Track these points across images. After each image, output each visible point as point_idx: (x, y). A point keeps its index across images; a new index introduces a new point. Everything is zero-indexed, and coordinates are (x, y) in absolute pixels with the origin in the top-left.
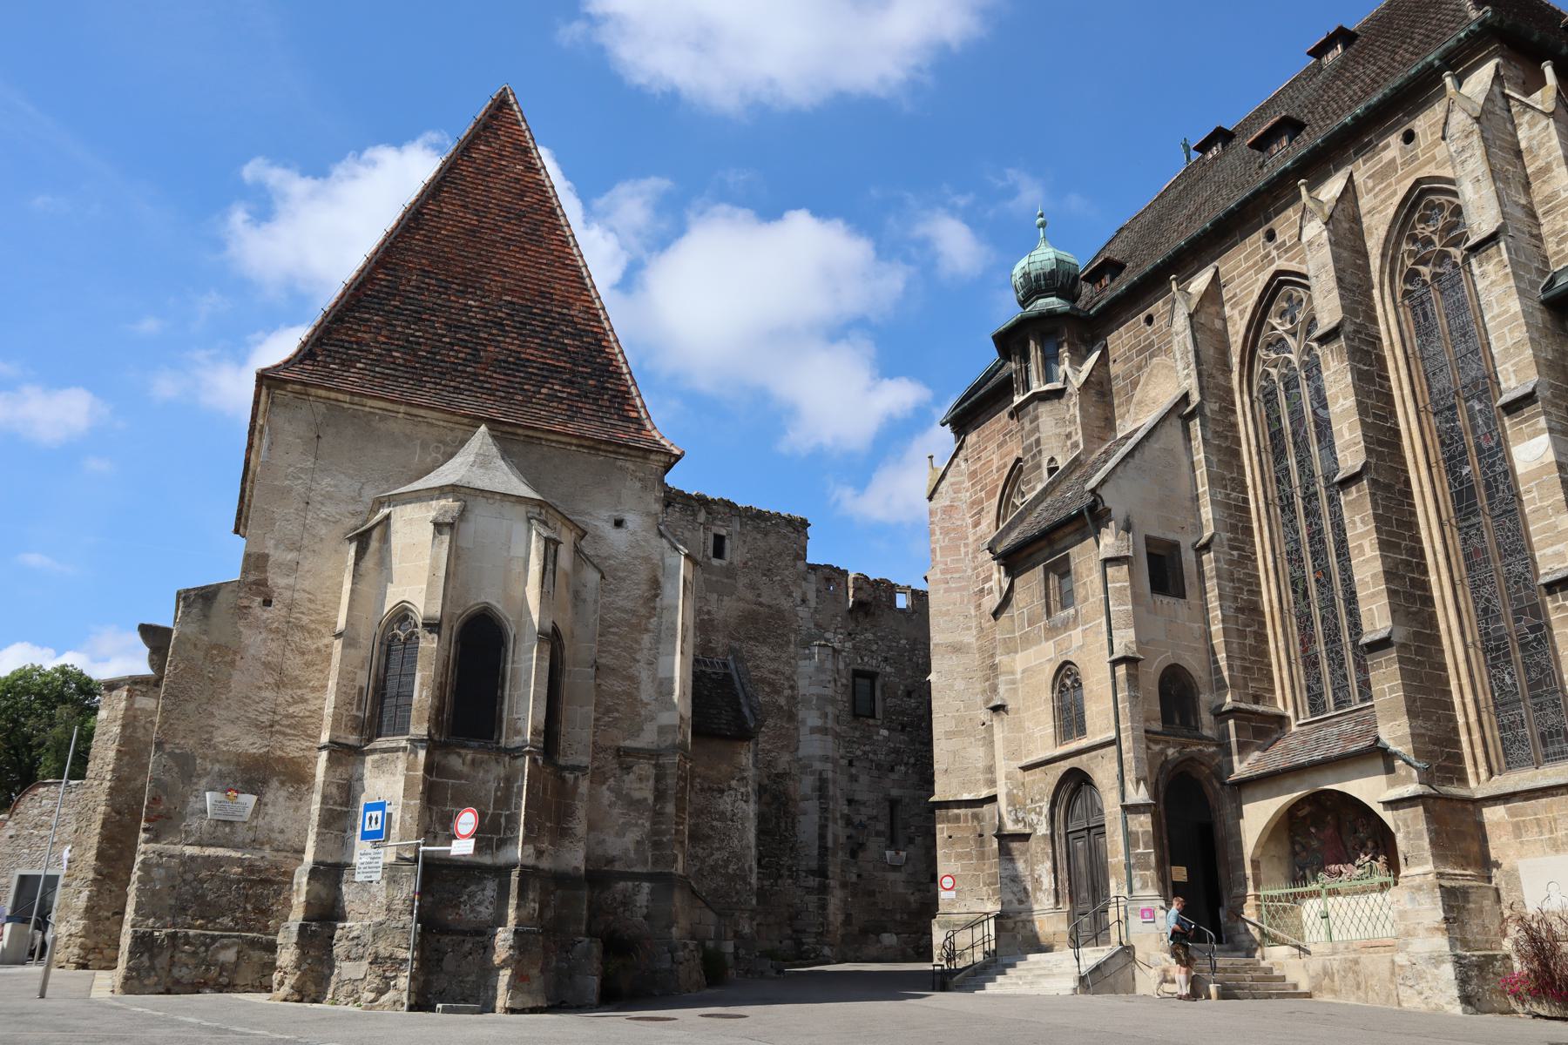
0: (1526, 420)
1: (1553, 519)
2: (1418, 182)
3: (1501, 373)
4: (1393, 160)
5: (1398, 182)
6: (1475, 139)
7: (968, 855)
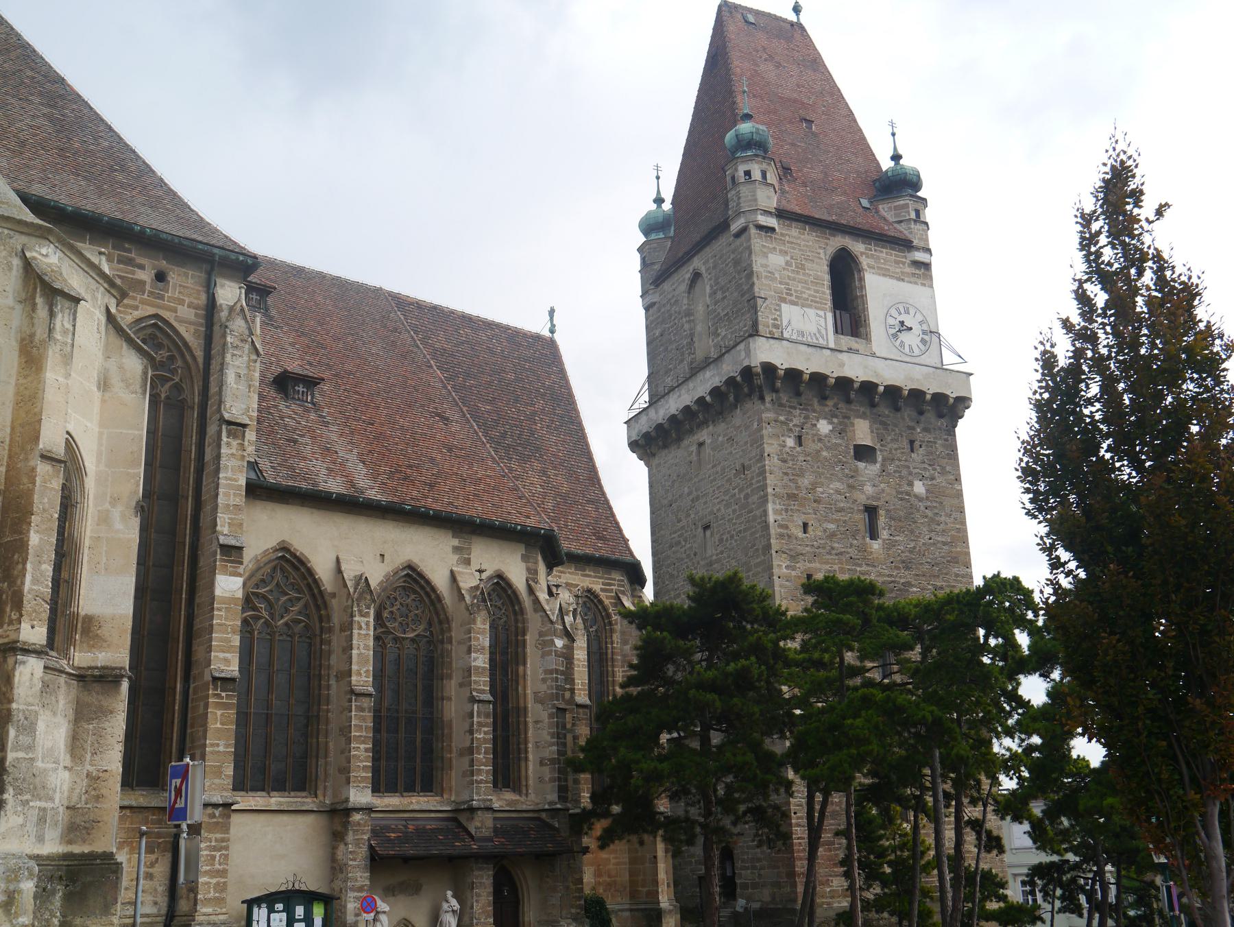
0: (232, 562)
1: (230, 635)
2: (156, 316)
3: (220, 518)
4: (143, 283)
5: (143, 302)
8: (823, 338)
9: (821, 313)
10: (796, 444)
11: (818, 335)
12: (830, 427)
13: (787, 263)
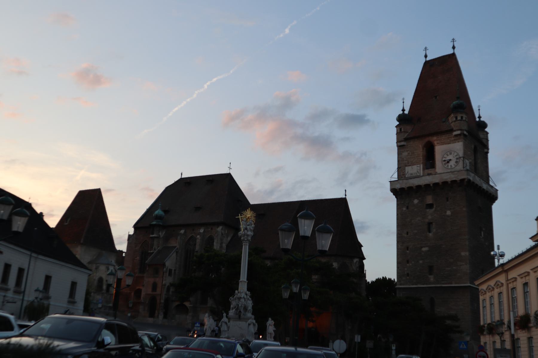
8: (419, 173)
9: (419, 165)
11: (417, 173)
12: (418, 201)
13: (408, 154)
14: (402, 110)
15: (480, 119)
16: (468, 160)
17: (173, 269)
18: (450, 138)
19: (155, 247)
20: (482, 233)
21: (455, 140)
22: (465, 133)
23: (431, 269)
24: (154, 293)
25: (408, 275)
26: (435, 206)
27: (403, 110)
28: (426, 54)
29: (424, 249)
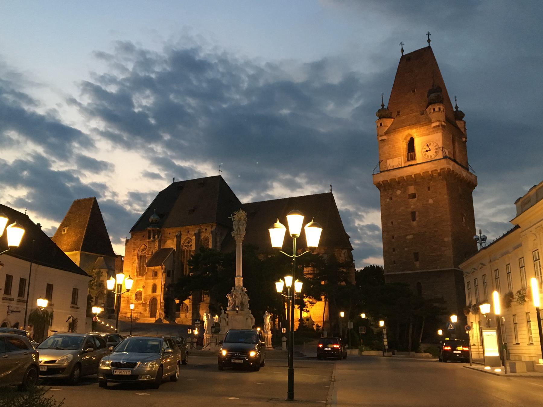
4: (204, 231)
6: (212, 238)
7: (126, 303)
8: (400, 165)
9: (400, 158)
10: (390, 200)
12: (401, 192)
14: (381, 106)
15: (457, 110)
16: (447, 150)
17: (171, 270)
18: (429, 130)
19: (152, 251)
20: (464, 218)
21: (433, 131)
22: (443, 123)
23: (416, 255)
24: (154, 294)
25: (394, 262)
26: (417, 196)
27: (383, 105)
28: (402, 48)
29: (408, 237)
